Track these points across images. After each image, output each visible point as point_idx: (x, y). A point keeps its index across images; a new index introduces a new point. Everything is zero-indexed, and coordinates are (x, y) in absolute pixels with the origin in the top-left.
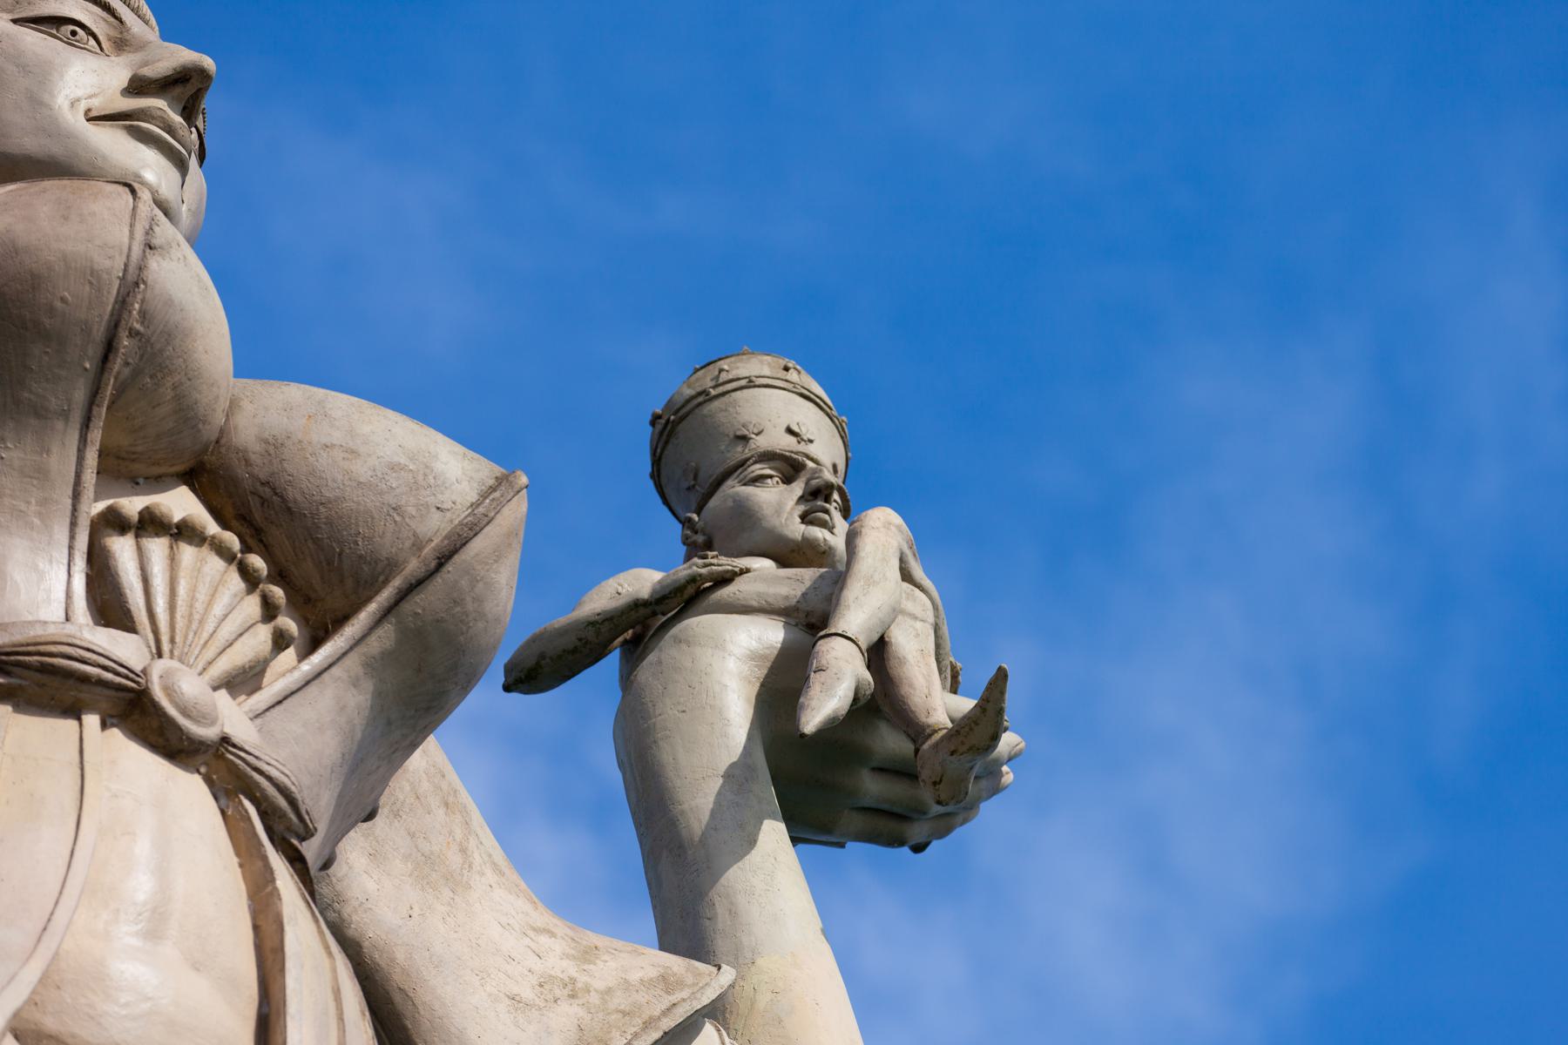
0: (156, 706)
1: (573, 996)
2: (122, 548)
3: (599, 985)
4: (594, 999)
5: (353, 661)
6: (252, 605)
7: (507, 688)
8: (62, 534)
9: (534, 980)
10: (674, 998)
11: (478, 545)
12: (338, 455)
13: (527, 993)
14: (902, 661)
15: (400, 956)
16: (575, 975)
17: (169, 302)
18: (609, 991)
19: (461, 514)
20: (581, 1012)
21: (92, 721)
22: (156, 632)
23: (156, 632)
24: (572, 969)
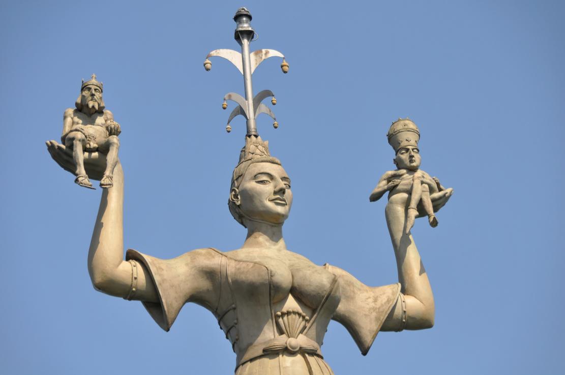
0: (289, 349)
1: (374, 311)
2: (280, 320)
3: (378, 307)
4: (377, 310)
5: (315, 324)
6: (301, 319)
7: (371, 201)
8: (270, 320)
9: (368, 310)
10: (389, 305)
11: (332, 293)
12: (309, 286)
13: (367, 313)
14: (424, 202)
15: (347, 315)
16: (374, 305)
17: (277, 283)
18: (379, 308)
19: (329, 291)
20: (375, 314)
21: (281, 356)
22: (287, 332)
23: (287, 332)
24: (372, 305)
